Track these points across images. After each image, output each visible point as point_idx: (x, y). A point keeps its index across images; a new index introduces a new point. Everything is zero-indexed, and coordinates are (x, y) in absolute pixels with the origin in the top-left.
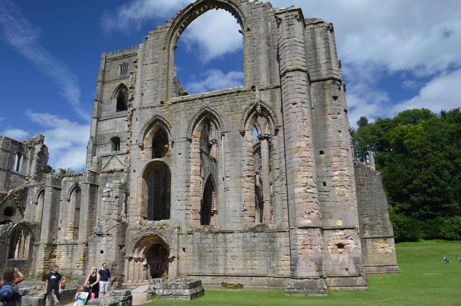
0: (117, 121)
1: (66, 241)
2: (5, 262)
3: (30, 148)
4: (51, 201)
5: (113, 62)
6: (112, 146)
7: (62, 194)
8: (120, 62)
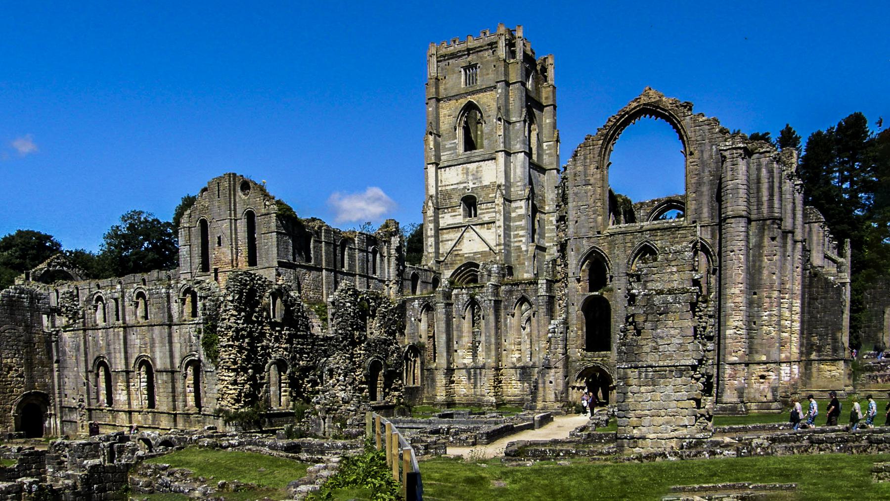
0: (468, 169)
3: (385, 242)
7: (454, 310)
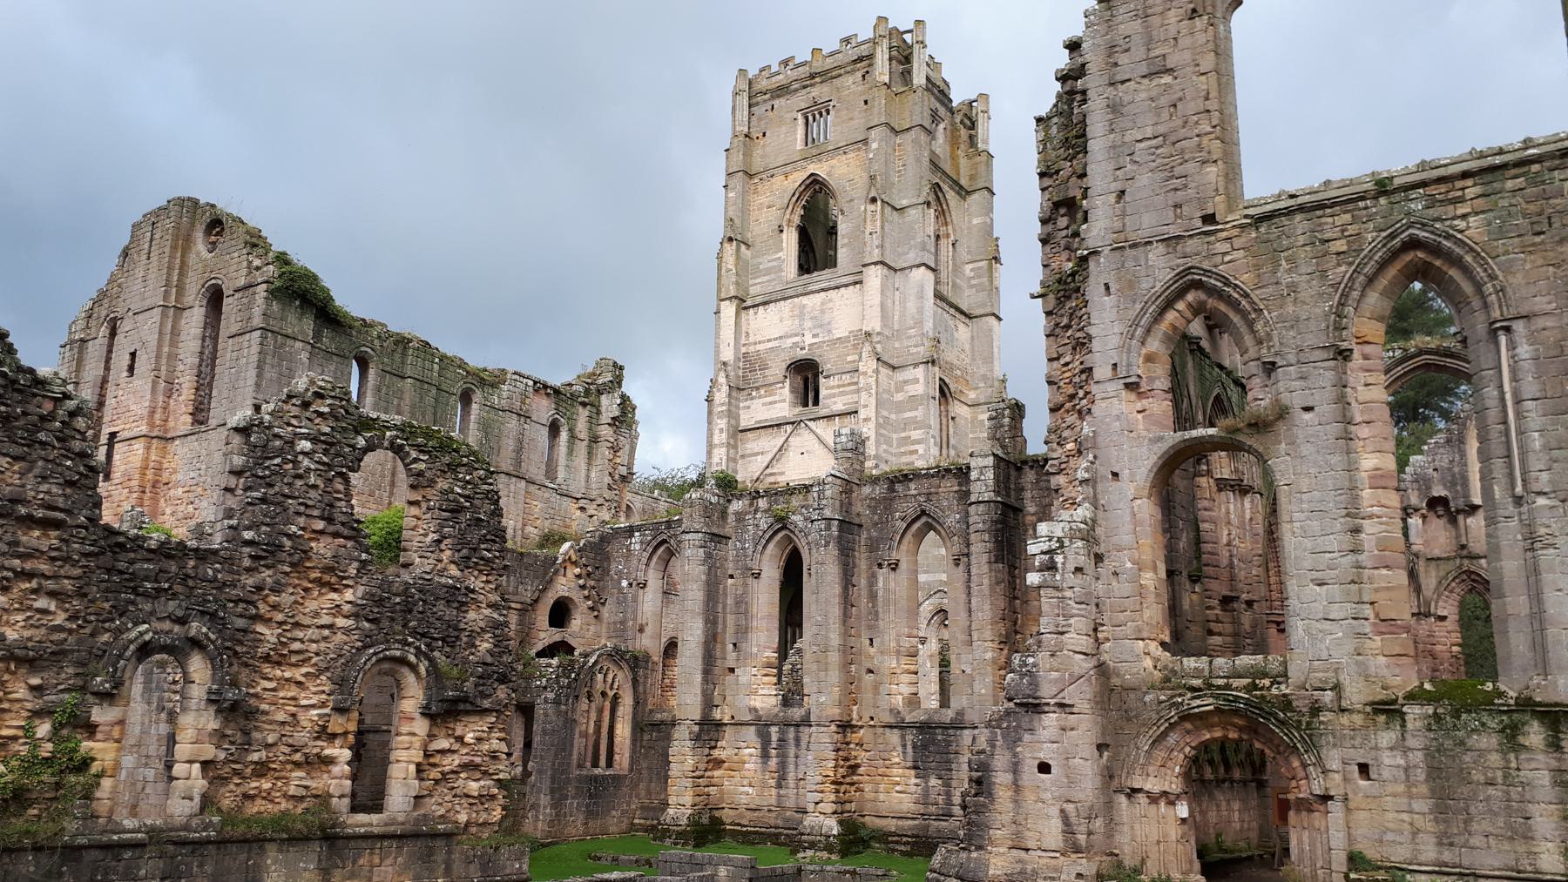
1: (756, 710)
2: (568, 781)
4: (704, 577)
5: (776, 103)
6: (793, 390)
8: (801, 100)
